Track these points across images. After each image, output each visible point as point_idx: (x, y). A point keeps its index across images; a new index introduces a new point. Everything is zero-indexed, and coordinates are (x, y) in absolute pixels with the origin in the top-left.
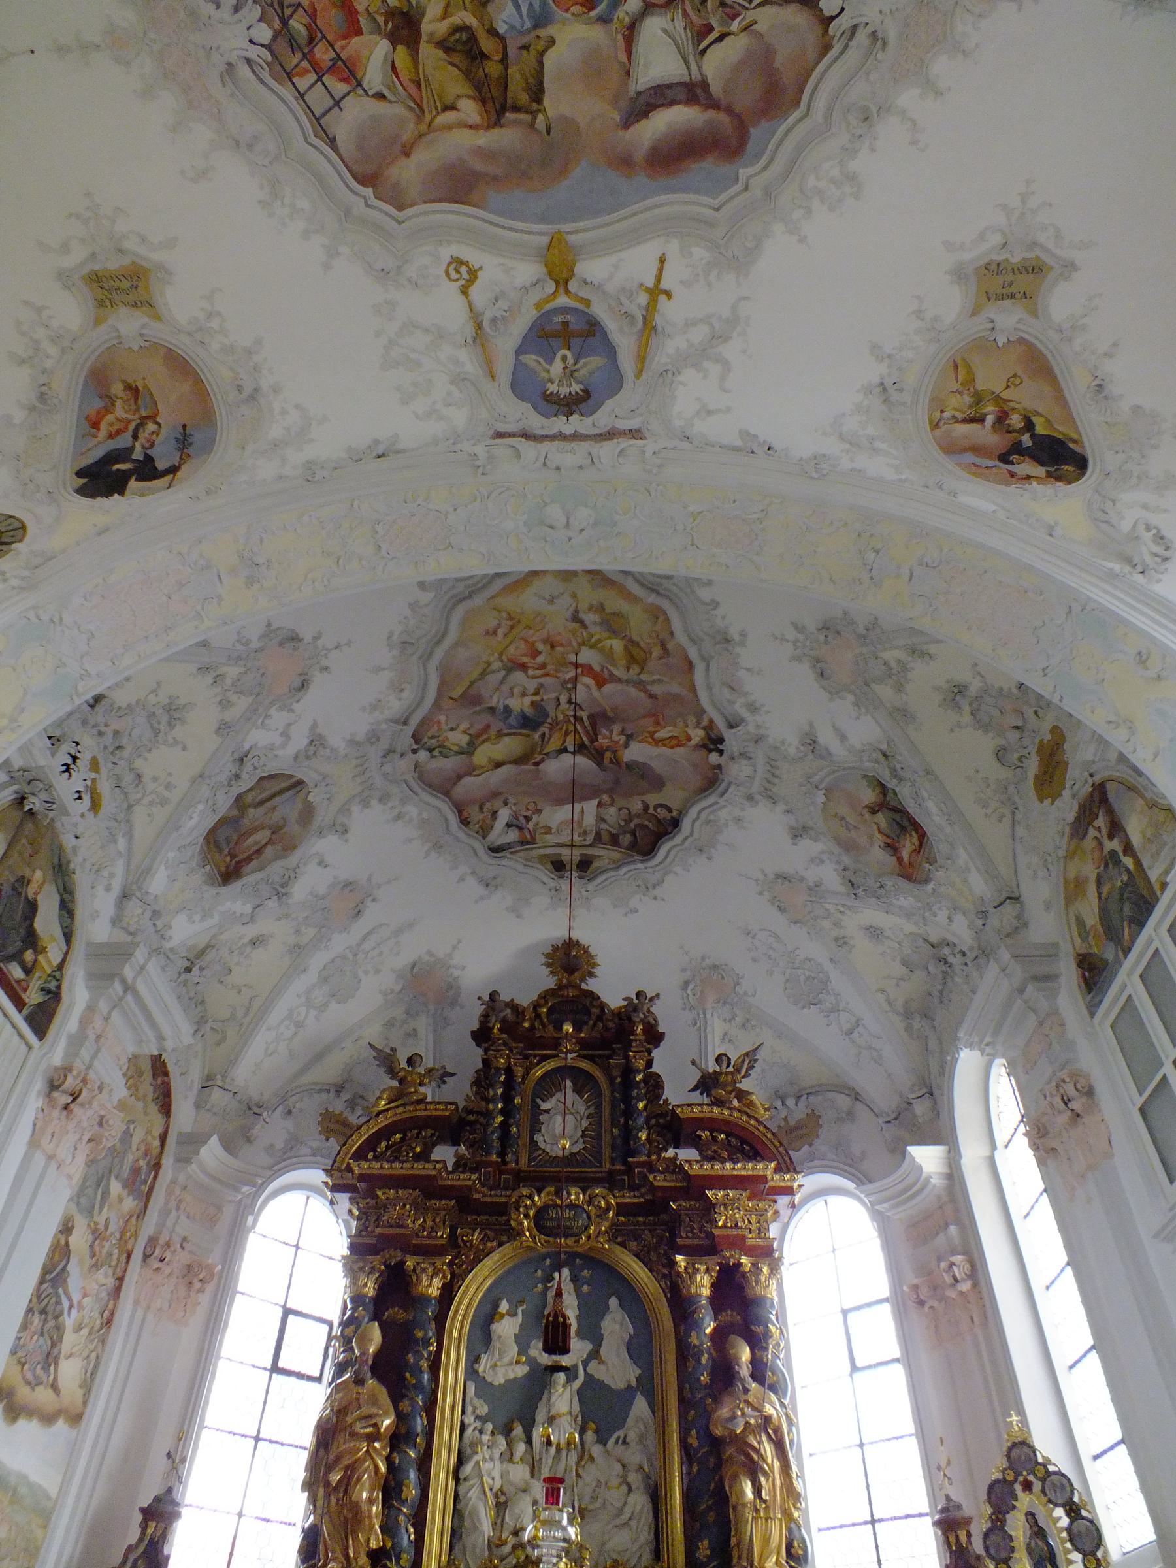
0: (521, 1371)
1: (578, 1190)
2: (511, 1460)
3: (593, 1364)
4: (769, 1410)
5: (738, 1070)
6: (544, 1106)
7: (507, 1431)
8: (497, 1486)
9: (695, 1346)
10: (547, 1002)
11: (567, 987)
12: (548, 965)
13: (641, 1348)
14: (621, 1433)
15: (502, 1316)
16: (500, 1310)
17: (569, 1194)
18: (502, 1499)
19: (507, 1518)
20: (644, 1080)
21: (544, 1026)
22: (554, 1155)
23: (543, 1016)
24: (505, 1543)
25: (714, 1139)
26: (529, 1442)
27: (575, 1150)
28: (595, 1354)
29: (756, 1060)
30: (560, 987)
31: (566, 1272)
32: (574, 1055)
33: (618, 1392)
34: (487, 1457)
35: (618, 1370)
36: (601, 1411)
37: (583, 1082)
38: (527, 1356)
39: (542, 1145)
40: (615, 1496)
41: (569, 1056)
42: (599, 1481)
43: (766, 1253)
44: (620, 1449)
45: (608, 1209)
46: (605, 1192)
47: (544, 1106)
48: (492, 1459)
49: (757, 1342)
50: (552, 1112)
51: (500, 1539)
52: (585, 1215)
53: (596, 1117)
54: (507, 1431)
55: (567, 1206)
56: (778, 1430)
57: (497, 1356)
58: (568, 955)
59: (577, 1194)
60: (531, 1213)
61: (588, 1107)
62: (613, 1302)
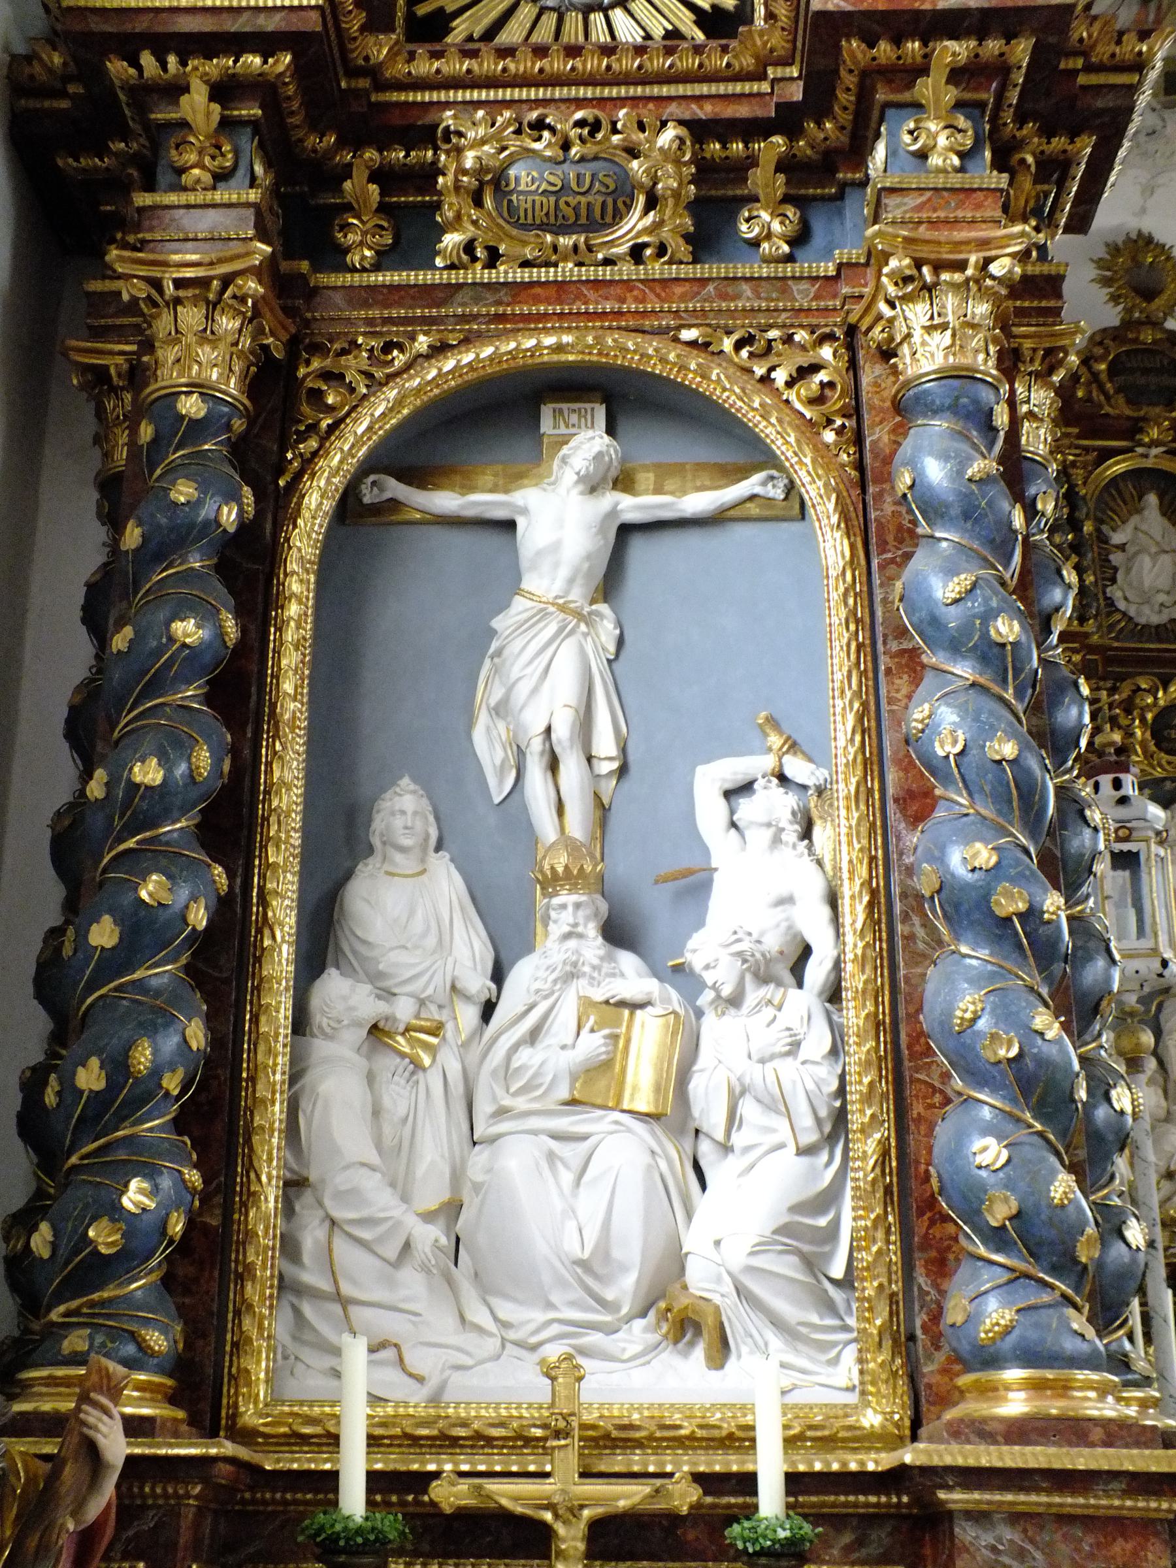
6: (1117, 538)
10: (1107, 351)
11: (1140, 323)
12: (1106, 282)
21: (1108, 398)
22: (1143, 620)
23: (1104, 377)
30: (1128, 324)
32: (1162, 449)
39: (1122, 605)
41: (1155, 451)
50: (1131, 549)
58: (1137, 264)
60: (1149, 716)
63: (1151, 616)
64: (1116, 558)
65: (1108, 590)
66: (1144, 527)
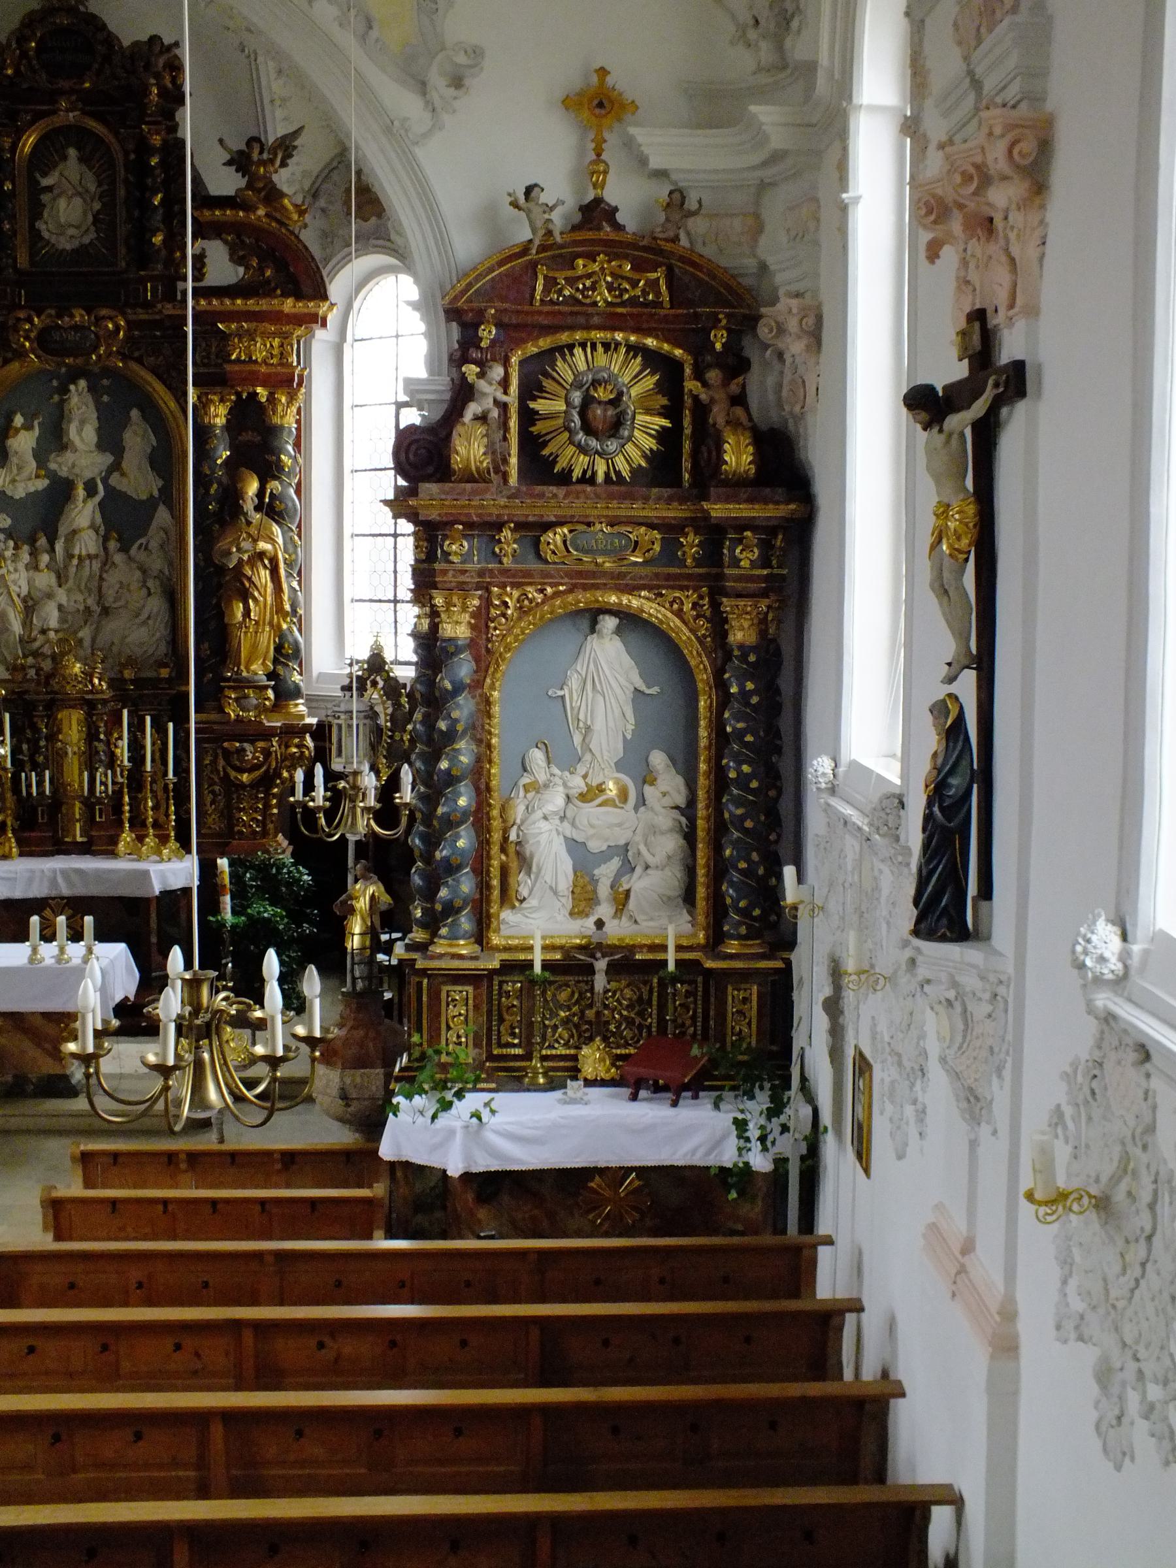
0: (42, 484)
1: (83, 313)
2: (36, 568)
3: (116, 475)
4: (263, 546)
5: (272, 161)
6: (46, 182)
7: (32, 541)
8: (24, 592)
9: (206, 475)
13: (164, 460)
14: (143, 540)
15: (17, 431)
16: (14, 424)
17: (72, 316)
18: (30, 603)
19: (35, 621)
20: (162, 162)
22: (60, 247)
24: (35, 640)
25: (243, 242)
26: (52, 550)
27: (86, 240)
28: (116, 467)
29: (295, 147)
31: (82, 383)
33: (142, 502)
34: (11, 569)
35: (139, 481)
36: (124, 520)
37: (93, 152)
38: (47, 469)
39: (46, 235)
40: (136, 596)
42: (121, 583)
43: (288, 381)
44: (141, 556)
45: (117, 328)
46: (113, 313)
47: (46, 182)
48: (16, 570)
49: (269, 470)
51: (29, 636)
52: (93, 336)
53: (108, 197)
54: (32, 541)
55: (71, 328)
56: (274, 561)
57: (15, 471)
59: (82, 316)
60: (33, 335)
61: (100, 185)
62: (135, 413)
63: (65, 244)
64: (45, 198)
65: (37, 224)
66: (66, 173)
